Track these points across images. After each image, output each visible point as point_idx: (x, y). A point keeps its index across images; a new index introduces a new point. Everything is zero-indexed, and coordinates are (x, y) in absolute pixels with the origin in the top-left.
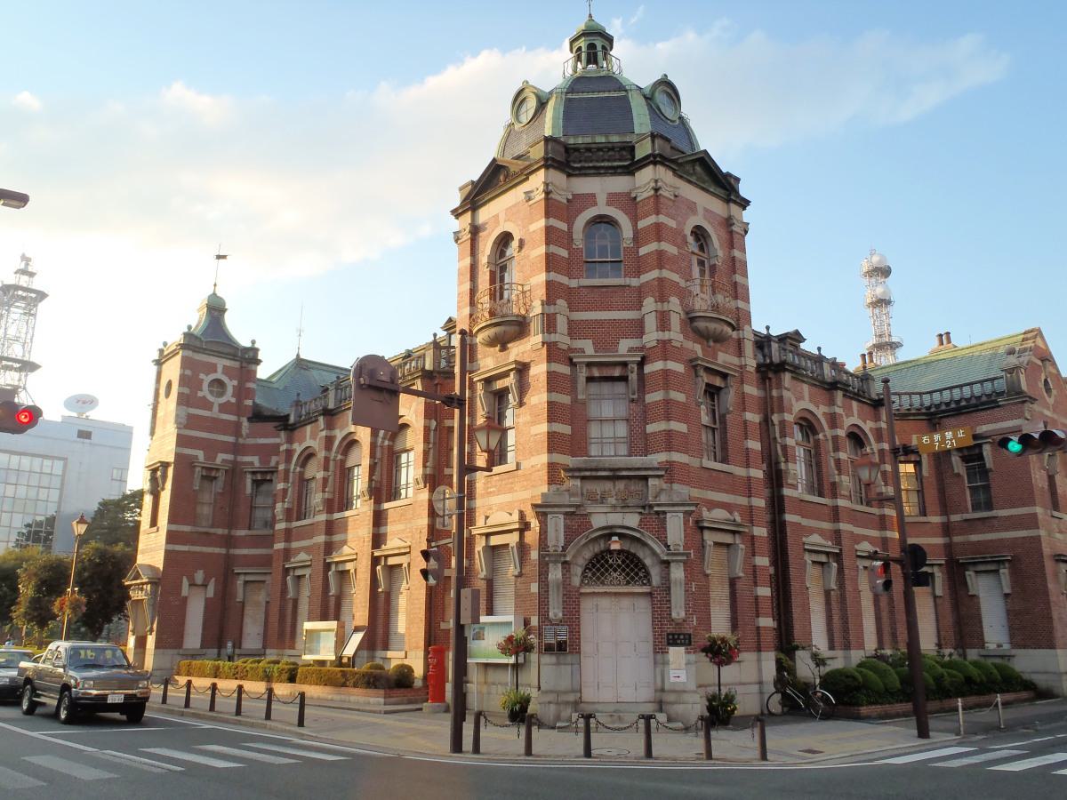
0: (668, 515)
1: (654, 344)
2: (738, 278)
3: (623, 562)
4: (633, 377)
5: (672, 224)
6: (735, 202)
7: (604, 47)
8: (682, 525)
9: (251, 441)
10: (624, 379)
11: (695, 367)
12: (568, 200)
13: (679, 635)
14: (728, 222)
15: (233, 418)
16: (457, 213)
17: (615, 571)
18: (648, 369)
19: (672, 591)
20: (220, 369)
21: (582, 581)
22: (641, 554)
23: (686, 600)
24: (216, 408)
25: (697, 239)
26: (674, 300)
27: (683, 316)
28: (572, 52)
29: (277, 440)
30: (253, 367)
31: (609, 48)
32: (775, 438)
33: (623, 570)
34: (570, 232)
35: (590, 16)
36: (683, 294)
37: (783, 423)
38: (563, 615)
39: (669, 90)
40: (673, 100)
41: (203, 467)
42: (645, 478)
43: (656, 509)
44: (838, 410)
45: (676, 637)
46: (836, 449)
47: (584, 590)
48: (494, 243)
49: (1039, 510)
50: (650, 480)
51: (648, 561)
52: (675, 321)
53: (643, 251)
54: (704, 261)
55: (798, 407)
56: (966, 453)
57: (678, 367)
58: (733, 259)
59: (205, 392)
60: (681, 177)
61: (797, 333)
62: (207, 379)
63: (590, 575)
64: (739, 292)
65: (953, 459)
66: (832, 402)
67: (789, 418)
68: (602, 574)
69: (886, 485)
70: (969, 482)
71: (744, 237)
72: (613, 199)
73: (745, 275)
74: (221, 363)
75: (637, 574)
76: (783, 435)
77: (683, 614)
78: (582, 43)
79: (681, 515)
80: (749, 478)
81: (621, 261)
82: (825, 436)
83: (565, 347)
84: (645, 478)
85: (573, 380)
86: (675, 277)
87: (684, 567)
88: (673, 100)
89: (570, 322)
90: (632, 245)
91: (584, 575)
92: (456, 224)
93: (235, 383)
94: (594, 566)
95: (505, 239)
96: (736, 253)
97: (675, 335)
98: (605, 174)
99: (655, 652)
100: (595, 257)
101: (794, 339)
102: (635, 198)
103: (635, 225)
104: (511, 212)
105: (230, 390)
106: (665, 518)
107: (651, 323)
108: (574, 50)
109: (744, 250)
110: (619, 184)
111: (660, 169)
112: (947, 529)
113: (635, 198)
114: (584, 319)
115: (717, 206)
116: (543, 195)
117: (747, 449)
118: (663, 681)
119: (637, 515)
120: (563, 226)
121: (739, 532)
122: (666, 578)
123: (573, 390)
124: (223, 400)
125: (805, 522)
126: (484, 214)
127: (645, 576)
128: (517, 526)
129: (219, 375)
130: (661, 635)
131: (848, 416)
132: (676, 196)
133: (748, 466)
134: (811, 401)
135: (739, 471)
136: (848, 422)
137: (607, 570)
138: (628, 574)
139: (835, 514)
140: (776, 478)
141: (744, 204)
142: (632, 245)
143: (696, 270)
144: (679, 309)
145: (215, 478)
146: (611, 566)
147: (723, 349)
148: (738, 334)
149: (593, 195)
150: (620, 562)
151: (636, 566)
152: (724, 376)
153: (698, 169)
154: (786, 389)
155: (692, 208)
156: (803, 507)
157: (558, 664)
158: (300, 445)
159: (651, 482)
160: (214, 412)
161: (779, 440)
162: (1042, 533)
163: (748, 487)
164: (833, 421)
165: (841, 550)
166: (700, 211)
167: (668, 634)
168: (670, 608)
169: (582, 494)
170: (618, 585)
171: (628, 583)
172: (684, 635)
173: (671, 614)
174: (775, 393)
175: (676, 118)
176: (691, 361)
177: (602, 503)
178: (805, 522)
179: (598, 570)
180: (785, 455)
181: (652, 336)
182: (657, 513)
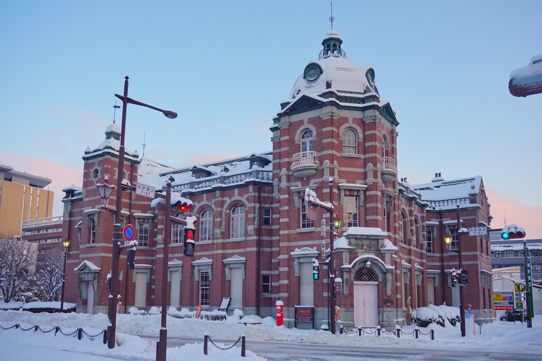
0: (386, 254)
1: (372, 184)
3: (368, 272)
4: (362, 196)
9: (137, 202)
12: (338, 119)
13: (388, 300)
17: (365, 275)
18: (368, 193)
30: (136, 165)
39: (372, 73)
42: (378, 240)
44: (413, 209)
47: (355, 282)
49: (478, 253)
50: (379, 240)
51: (378, 272)
53: (367, 144)
56: (452, 228)
65: (447, 230)
66: (410, 205)
68: (360, 276)
69: (424, 240)
72: (355, 120)
75: (372, 277)
79: (390, 255)
98: (352, 110)
99: (379, 306)
102: (364, 122)
106: (384, 255)
111: (376, 111)
112: (442, 259)
113: (364, 122)
117: (395, 226)
127: (375, 278)
137: (362, 275)
138: (369, 277)
141: (397, 124)
142: (362, 141)
146: (363, 273)
147: (390, 185)
149: (347, 118)
150: (366, 272)
151: (372, 274)
157: (346, 311)
162: (478, 262)
165: (411, 267)
167: (385, 300)
170: (366, 281)
171: (369, 280)
177: (362, 248)
181: (370, 179)
182: (382, 254)
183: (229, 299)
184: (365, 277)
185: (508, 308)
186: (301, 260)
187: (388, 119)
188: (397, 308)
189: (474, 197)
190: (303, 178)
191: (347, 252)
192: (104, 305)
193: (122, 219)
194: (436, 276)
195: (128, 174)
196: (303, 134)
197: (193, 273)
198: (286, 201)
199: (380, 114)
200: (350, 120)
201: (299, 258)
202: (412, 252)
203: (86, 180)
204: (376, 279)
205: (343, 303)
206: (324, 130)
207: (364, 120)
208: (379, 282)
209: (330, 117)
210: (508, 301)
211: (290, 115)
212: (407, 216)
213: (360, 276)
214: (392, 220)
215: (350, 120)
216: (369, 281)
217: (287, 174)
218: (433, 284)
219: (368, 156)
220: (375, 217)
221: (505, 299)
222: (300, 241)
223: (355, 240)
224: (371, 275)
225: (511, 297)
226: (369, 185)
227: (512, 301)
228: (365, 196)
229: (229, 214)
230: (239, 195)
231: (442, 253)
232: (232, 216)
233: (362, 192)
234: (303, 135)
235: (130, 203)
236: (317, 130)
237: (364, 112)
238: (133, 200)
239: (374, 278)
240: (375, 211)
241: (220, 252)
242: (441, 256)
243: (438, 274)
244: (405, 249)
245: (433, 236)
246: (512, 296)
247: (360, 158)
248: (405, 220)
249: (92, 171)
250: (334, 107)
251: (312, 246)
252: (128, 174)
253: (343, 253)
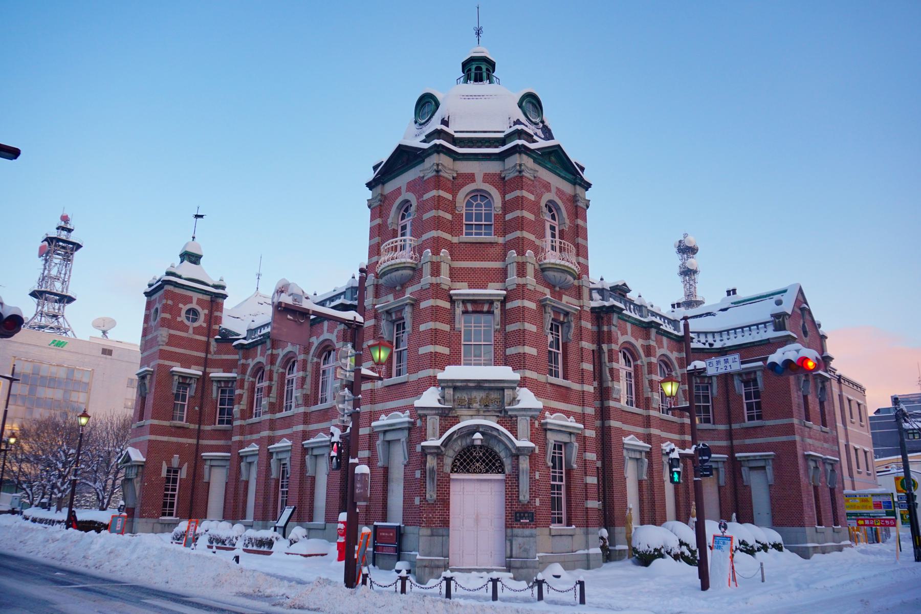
0: (519, 418)
2: (580, 240)
3: (484, 454)
4: (497, 312)
5: (531, 197)
6: (580, 185)
7: (487, 70)
8: (529, 427)
10: (490, 312)
11: (544, 306)
12: (454, 178)
14: (574, 199)
15: (204, 339)
16: (370, 185)
17: (478, 461)
18: (509, 305)
19: (520, 478)
20: (195, 301)
21: (452, 469)
22: (497, 449)
23: (530, 486)
24: (191, 331)
25: (550, 211)
26: (529, 253)
27: (537, 267)
28: (464, 73)
29: (237, 357)
30: (220, 300)
31: (491, 71)
32: (605, 362)
33: (484, 461)
34: (453, 202)
36: (537, 250)
37: (610, 351)
38: (437, 496)
40: (537, 108)
41: (179, 376)
42: (503, 389)
43: (510, 413)
44: (653, 343)
45: (522, 515)
46: (650, 372)
47: (454, 476)
48: (397, 208)
49: (795, 421)
50: (506, 390)
51: (502, 455)
52: (530, 270)
53: (509, 217)
54: (555, 227)
55: (622, 339)
56: (744, 377)
57: (532, 305)
58: (577, 226)
59: (183, 318)
60: (539, 164)
61: (625, 285)
62: (184, 308)
63: (458, 464)
64: (582, 251)
65: (735, 382)
66: (648, 337)
67: (615, 347)
68: (468, 464)
70: (746, 400)
71: (586, 210)
72: (487, 178)
73: (586, 239)
74: (196, 296)
75: (494, 464)
76: (611, 360)
77: (527, 497)
79: (528, 418)
80: (583, 392)
81: (491, 225)
82: (642, 362)
83: (447, 288)
84: (503, 389)
85: (452, 312)
86: (532, 237)
87: (530, 459)
88: (537, 108)
89: (451, 269)
90: (500, 212)
91: (454, 465)
92: (369, 194)
93: (206, 311)
94: (462, 457)
95: (405, 206)
96: (580, 222)
97: (530, 280)
99: (506, 527)
100: (472, 221)
101: (620, 291)
102: (504, 178)
103: (503, 198)
104: (411, 187)
105: (202, 318)
106: (517, 420)
107: (512, 270)
108: (465, 72)
109: (585, 220)
110: (494, 167)
111: (524, 157)
112: (730, 435)
113: (504, 178)
114: (462, 267)
115: (567, 188)
117: (582, 369)
118: (511, 550)
119: (495, 417)
120: (449, 197)
121: (573, 433)
122: (516, 467)
123: (452, 321)
124: (196, 324)
125: (626, 427)
126: (390, 187)
127: (500, 466)
129: (194, 305)
130: (511, 513)
131: (659, 348)
132: (535, 177)
133: (582, 382)
134: (632, 335)
135: (576, 387)
136: (659, 352)
137: (471, 461)
138: (487, 464)
139: (647, 422)
140: (604, 393)
141: (587, 186)
142: (500, 212)
143: (548, 232)
144: (533, 260)
145: (189, 385)
146: (475, 457)
147: (566, 293)
148: (579, 282)
149: (473, 175)
150: (481, 454)
151: (494, 458)
152: (567, 314)
153: (553, 158)
154: (613, 325)
155: (547, 187)
156: (624, 416)
157: (432, 535)
158: (253, 360)
159: (507, 392)
160: (190, 334)
161: (608, 364)
162: (797, 438)
163: (582, 399)
164: (648, 351)
165: (651, 449)
166: (553, 190)
168: (518, 491)
169: (454, 401)
170: (480, 473)
171: (487, 472)
172: (529, 513)
173: (518, 497)
174: (605, 328)
175: (538, 120)
176: (541, 301)
177: (469, 408)
178: (626, 427)
179: (465, 460)
180: (612, 376)
181: (513, 279)
182: (511, 417)
183: (292, 509)
184: (478, 465)
185: (884, 522)
186: (390, 437)
187: (562, 174)
188: (587, 527)
189: (781, 320)
190: (395, 287)
191: (435, 414)
192: (148, 517)
193: (191, 382)
194: (720, 465)
195: (205, 314)
196: (402, 212)
197: (269, 465)
198: (372, 330)
199: (535, 161)
200: (479, 178)
201: (385, 432)
202: (653, 422)
203: (146, 325)
204: (500, 469)
205: (425, 518)
206: (426, 196)
207: (503, 175)
208: (506, 475)
209: (434, 173)
210: (884, 510)
211: (383, 184)
212: (640, 357)
213: (468, 464)
214: (573, 357)
215: (479, 178)
216: (485, 473)
217: (375, 283)
218: (715, 481)
219: (510, 237)
220: (520, 349)
221: (877, 505)
222: (388, 400)
223: (454, 391)
224: (490, 461)
225: (890, 502)
226: (511, 290)
227: (893, 509)
228: (503, 310)
229: (318, 364)
230: (328, 331)
231: (730, 424)
232: (323, 367)
233: (497, 305)
234: (403, 214)
235: (206, 359)
236: (418, 199)
237: (504, 161)
238: (213, 353)
239: (496, 467)
240: (521, 338)
241: (300, 428)
242: (728, 428)
243: (724, 462)
244: (637, 416)
245: (712, 394)
246: (891, 500)
247: (497, 243)
248: (636, 363)
249: (153, 311)
250: (442, 155)
251: (402, 410)
252: (205, 314)
253: (428, 417)
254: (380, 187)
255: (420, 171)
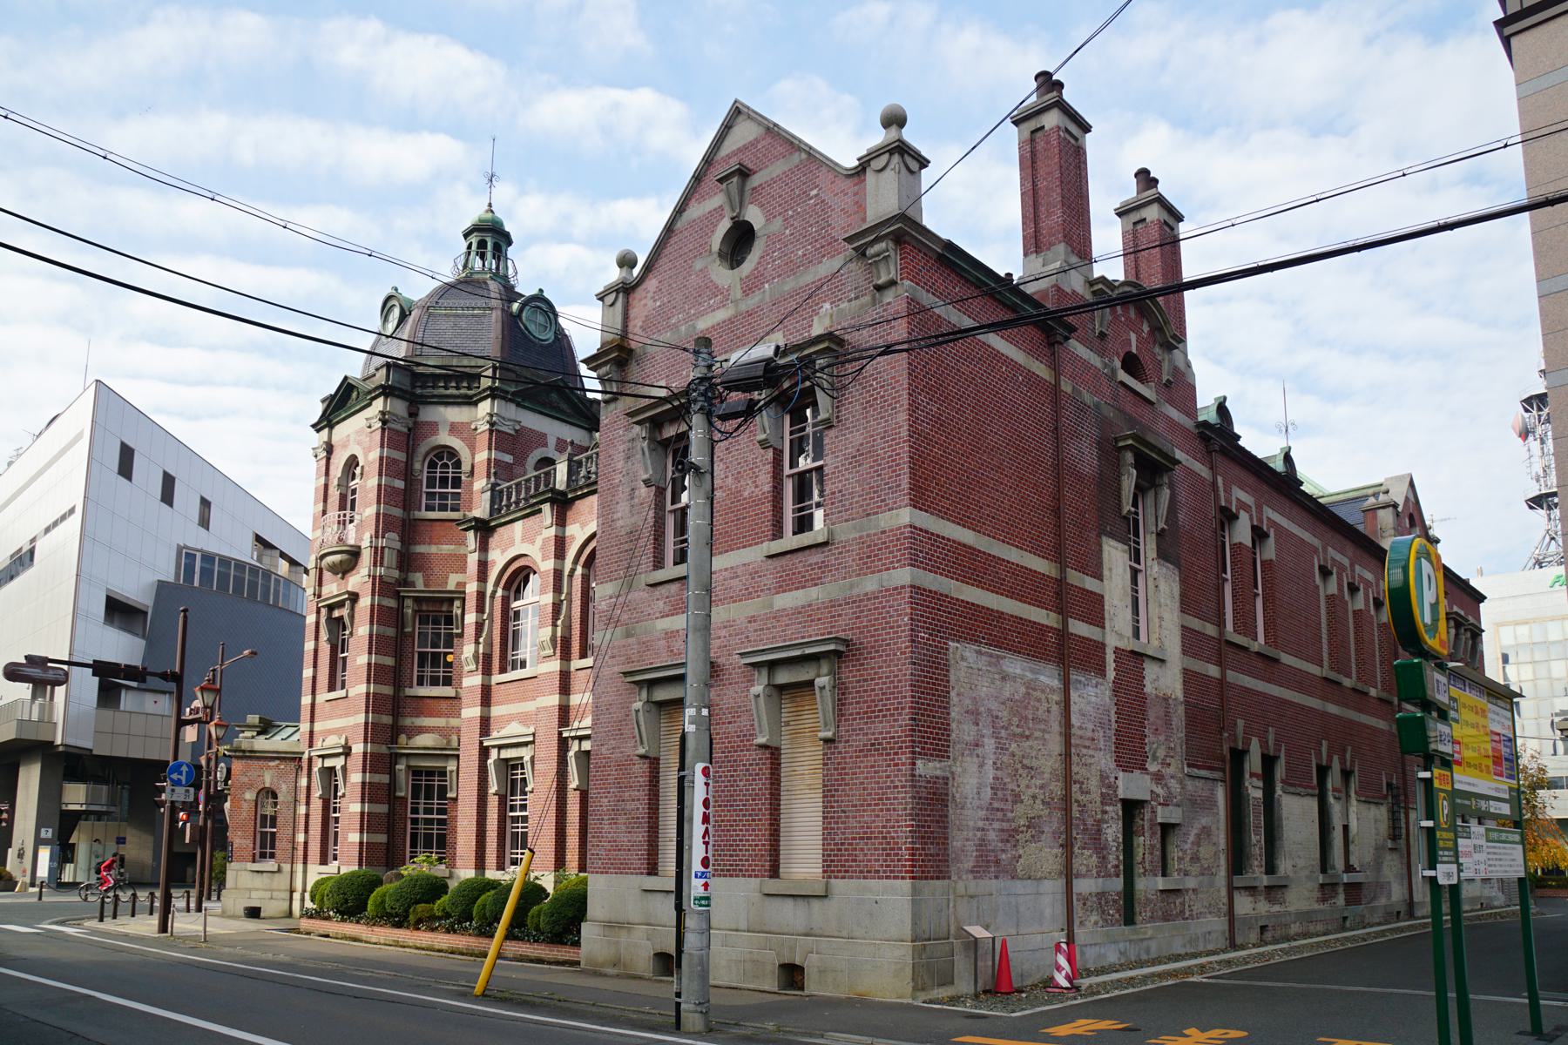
16: (317, 427)
35: (490, 205)
78: (474, 240)
102: (476, 429)
113: (476, 429)
116: (380, 424)
128: (341, 750)
155: (541, 439)
166: (552, 442)
211: (331, 426)
254: (326, 431)
255: (367, 419)
